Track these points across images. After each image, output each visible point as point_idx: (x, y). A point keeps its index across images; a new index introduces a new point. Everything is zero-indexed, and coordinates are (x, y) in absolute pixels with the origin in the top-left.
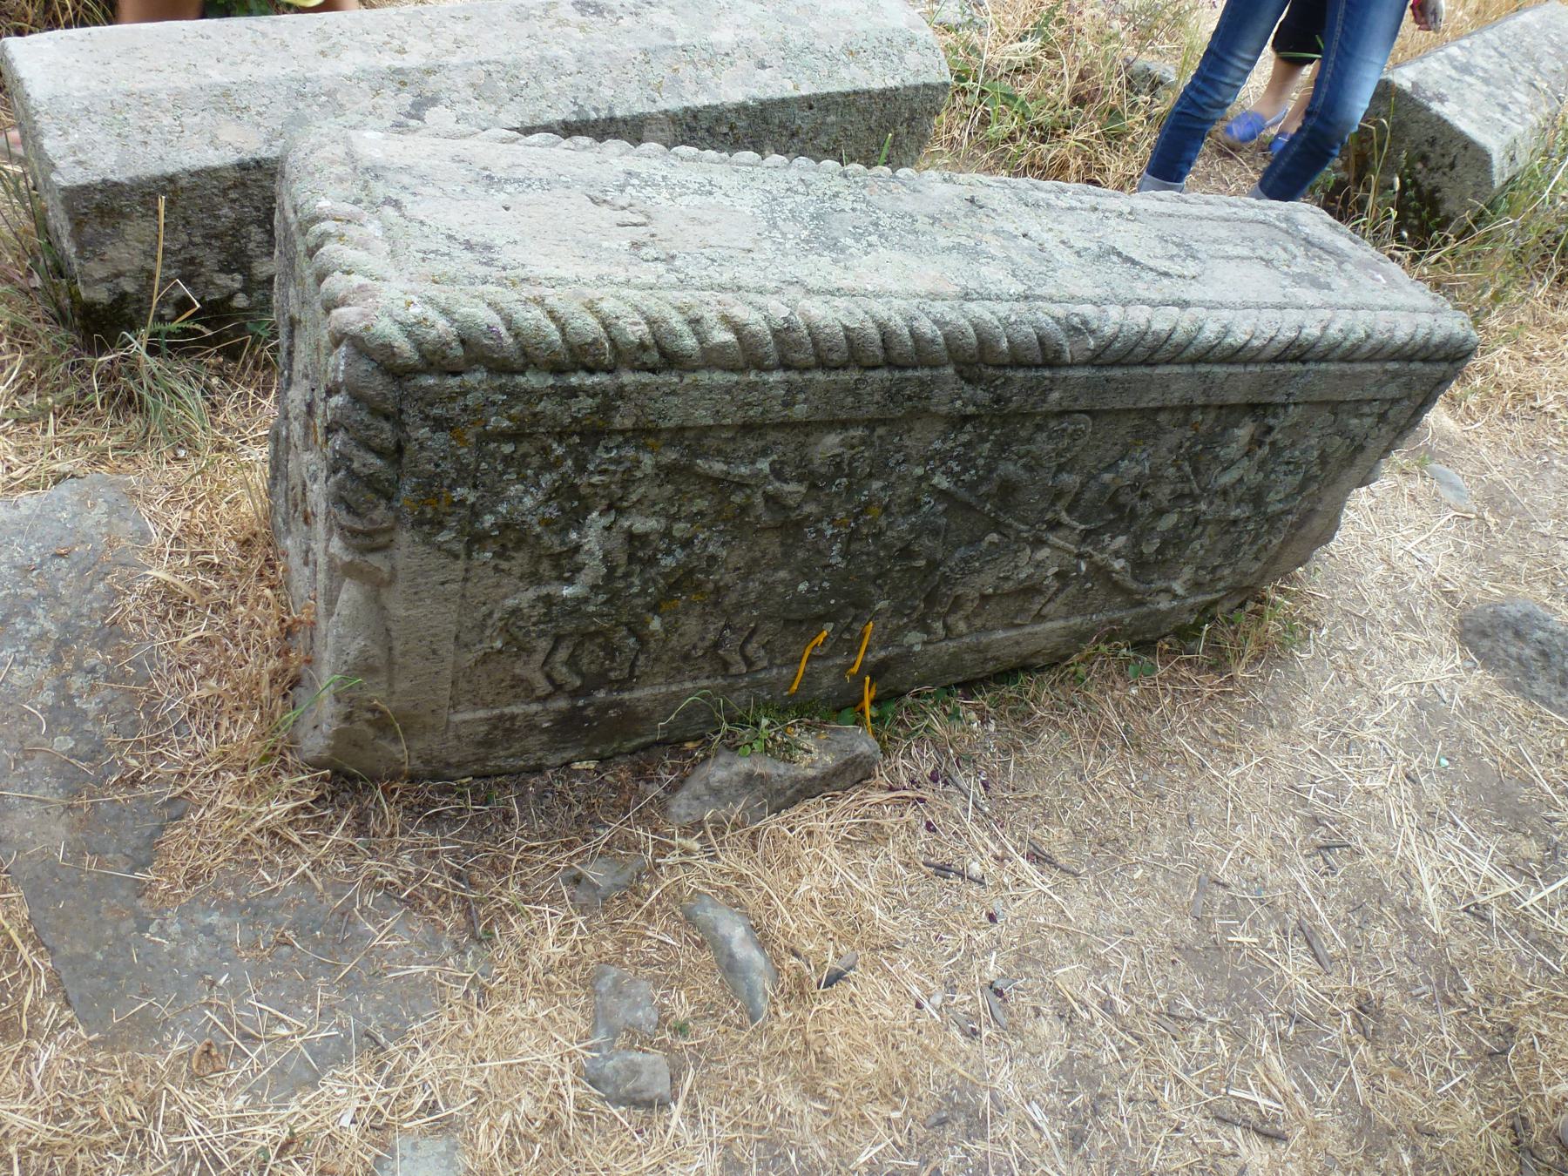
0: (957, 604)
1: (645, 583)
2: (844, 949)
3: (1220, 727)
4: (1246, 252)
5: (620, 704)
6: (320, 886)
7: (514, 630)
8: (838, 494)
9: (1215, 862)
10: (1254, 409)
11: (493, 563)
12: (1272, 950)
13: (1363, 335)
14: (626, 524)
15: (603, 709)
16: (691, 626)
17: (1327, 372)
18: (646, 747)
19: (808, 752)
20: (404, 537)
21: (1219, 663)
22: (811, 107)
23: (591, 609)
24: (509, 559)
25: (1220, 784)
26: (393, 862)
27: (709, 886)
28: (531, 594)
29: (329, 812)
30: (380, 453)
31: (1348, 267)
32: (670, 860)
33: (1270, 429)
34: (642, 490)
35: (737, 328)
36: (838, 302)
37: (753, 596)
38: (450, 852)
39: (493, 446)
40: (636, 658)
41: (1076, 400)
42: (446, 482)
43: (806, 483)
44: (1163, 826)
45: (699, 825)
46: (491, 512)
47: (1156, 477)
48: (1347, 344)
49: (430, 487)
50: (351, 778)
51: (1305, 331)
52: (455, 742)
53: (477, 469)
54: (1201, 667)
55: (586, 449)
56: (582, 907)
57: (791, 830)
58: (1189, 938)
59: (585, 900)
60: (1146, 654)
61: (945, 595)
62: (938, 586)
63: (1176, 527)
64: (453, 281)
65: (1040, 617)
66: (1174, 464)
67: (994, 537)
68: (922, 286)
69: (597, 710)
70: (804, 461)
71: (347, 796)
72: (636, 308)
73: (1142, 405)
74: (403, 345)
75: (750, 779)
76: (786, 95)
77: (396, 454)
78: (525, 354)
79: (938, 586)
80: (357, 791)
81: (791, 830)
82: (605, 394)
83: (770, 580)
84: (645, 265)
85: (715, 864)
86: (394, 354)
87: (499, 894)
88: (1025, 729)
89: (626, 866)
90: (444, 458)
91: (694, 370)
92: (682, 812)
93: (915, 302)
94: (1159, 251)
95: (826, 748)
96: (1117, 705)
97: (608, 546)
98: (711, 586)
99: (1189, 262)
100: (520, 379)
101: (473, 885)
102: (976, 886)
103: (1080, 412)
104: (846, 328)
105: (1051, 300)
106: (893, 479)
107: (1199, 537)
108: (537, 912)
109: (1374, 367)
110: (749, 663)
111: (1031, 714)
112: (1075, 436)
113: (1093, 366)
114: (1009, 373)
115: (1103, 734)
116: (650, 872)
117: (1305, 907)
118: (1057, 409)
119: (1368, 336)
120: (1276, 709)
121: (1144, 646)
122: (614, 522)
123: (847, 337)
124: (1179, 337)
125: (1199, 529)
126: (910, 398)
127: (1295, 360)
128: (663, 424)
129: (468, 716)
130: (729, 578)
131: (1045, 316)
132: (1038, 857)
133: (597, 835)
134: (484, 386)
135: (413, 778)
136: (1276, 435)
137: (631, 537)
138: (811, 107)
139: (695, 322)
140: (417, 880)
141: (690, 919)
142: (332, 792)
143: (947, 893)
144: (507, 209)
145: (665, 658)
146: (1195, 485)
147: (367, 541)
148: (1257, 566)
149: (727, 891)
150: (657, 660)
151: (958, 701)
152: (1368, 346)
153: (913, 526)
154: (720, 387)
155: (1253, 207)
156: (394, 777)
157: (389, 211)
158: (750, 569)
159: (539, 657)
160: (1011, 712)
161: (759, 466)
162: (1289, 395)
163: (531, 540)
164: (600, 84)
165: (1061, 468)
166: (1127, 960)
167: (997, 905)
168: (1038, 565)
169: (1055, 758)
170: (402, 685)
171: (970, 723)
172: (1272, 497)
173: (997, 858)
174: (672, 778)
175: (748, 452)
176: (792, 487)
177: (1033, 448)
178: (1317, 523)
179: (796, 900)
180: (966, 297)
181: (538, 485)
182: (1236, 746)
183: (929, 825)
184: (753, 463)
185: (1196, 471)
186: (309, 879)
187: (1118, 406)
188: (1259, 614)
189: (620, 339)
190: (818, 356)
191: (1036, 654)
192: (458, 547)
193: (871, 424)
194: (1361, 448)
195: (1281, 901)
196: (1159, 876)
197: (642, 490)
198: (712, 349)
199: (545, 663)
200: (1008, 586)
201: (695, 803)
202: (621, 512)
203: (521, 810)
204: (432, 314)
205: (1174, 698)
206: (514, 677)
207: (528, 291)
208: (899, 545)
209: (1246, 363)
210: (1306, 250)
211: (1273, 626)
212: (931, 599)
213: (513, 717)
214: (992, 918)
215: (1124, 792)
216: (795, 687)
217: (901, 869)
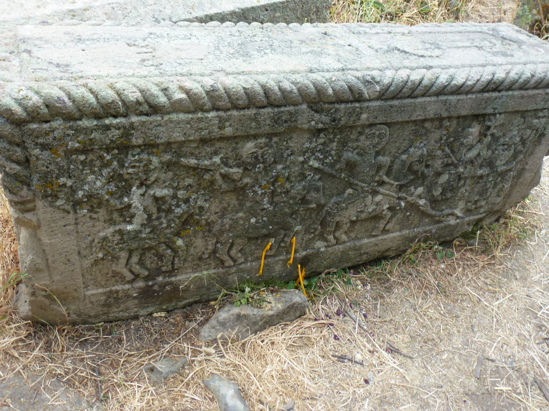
0: (338, 226)
1: (169, 221)
2: (288, 400)
3: (488, 281)
4: (468, 44)
5: (171, 283)
6: (25, 377)
7: (106, 248)
8: (260, 172)
9: (487, 349)
10: (478, 117)
11: (88, 215)
12: (520, 394)
13: (529, 75)
14: (152, 192)
15: (163, 286)
16: (199, 242)
17: (513, 96)
18: (190, 305)
19: (270, 303)
20: (40, 204)
21: (486, 250)
22: (267, 10)
23: (144, 236)
24: (96, 213)
25: (489, 309)
26: (62, 364)
27: (219, 370)
28: (111, 230)
29: (33, 341)
30: (18, 163)
31: (524, 47)
32: (199, 358)
33: (489, 128)
34: (156, 175)
35: (187, 92)
36: (241, 77)
37: (227, 226)
38: (90, 358)
39: (74, 157)
40: (174, 259)
41: (376, 118)
42: (54, 176)
43: (242, 168)
44: (459, 331)
45: (215, 340)
46: (81, 190)
47: (431, 155)
48: (521, 80)
49: (45, 177)
50: (44, 325)
51: (496, 76)
52: (90, 305)
53: (69, 168)
54: (477, 252)
55: (122, 156)
56: (154, 382)
57: (262, 341)
58: (473, 389)
59: (155, 379)
60: (449, 248)
61: (330, 221)
62: (326, 217)
63: (448, 181)
64: (46, 80)
65: (385, 231)
66: (440, 148)
67: (350, 191)
68: (287, 68)
69: (160, 286)
70: (238, 157)
71: (41, 333)
72: (135, 85)
73: (414, 118)
74: (17, 109)
75: (239, 317)
76: (254, 5)
77: (26, 162)
78: (80, 110)
79: (326, 217)
80: (47, 331)
81: (262, 341)
82: (124, 128)
83: (235, 218)
84: (145, 68)
85: (223, 360)
86: (13, 114)
87: (113, 378)
88: (386, 287)
89: (177, 362)
90: (50, 164)
91: (169, 113)
92: (206, 335)
93: (283, 75)
94: (420, 47)
95: (278, 300)
96: (433, 273)
97: (145, 204)
98: (204, 222)
99: (436, 50)
100: (80, 123)
101: (100, 374)
102: (359, 366)
103: (381, 124)
104: (244, 88)
105: (357, 70)
106: (288, 163)
107: (464, 185)
108: (131, 386)
109: (540, 91)
110: (235, 261)
111: (388, 280)
112: (381, 136)
113: (382, 100)
114: (337, 106)
115: (426, 288)
116: (189, 365)
117: (537, 370)
118: (367, 123)
119: (533, 76)
120: (519, 271)
121: (446, 244)
122: (146, 191)
123: (246, 93)
124: (425, 82)
125: (462, 182)
126: (286, 122)
127: (494, 90)
128: (159, 141)
129: (94, 292)
130: (213, 218)
131: (351, 77)
132: (391, 350)
133: (163, 347)
134: (62, 127)
135: (74, 324)
136: (493, 130)
137: (156, 199)
138: (267, 10)
139: (165, 90)
140: (73, 372)
141: (207, 387)
142: (35, 332)
143: (345, 369)
144: (83, 50)
145: (189, 259)
146: (454, 159)
147: (22, 207)
148: (499, 200)
149: (228, 373)
150: (185, 260)
151: (350, 275)
152: (533, 81)
153: (304, 188)
154: (183, 121)
155: (476, 26)
156: (64, 323)
157: (25, 55)
158: (223, 214)
159: (123, 261)
160: (378, 279)
161: (214, 160)
162: (494, 109)
163: (105, 203)
164: (165, 8)
165: (378, 154)
166: (439, 401)
167: (370, 375)
168: (377, 204)
169: (402, 301)
170: (56, 278)
171: (357, 285)
172: (498, 163)
173: (370, 351)
174: (202, 318)
175: (207, 153)
176: (235, 170)
177: (360, 144)
178: (528, 176)
179: (264, 376)
180: (311, 71)
181: (102, 175)
182: (497, 290)
183: (335, 336)
184: (211, 159)
185: (453, 151)
186: (21, 374)
187: (400, 120)
188: (506, 224)
189: (127, 100)
190: (232, 103)
191: (388, 250)
192: (68, 207)
193: (270, 136)
194: (543, 135)
195: (524, 368)
196: (456, 357)
197: (156, 175)
199: (127, 264)
200: (363, 216)
201: (213, 330)
202: (148, 187)
203: (127, 337)
204: (31, 94)
205: (464, 269)
206: (113, 272)
207: (83, 81)
208: (299, 197)
209: (467, 93)
210: (502, 42)
211: (514, 230)
212: (323, 224)
213: (117, 292)
214: (366, 381)
215: (437, 315)
216: (261, 271)
217: (320, 359)
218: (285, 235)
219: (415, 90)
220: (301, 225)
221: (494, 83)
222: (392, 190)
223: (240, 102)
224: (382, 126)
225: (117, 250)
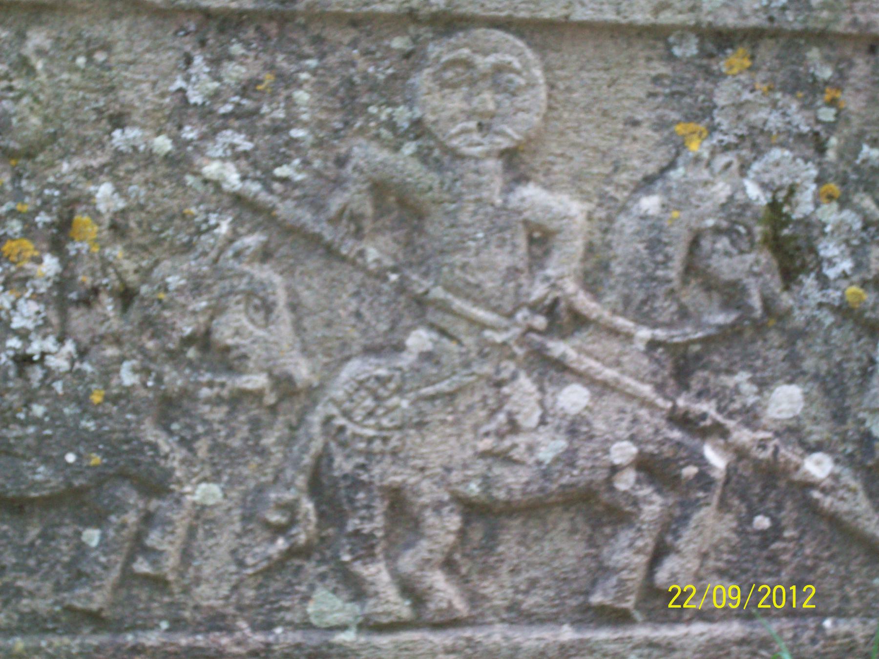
103: (495, 24)
218: (148, 519)
220: (215, 477)
222: (630, 367)
224: (498, 35)
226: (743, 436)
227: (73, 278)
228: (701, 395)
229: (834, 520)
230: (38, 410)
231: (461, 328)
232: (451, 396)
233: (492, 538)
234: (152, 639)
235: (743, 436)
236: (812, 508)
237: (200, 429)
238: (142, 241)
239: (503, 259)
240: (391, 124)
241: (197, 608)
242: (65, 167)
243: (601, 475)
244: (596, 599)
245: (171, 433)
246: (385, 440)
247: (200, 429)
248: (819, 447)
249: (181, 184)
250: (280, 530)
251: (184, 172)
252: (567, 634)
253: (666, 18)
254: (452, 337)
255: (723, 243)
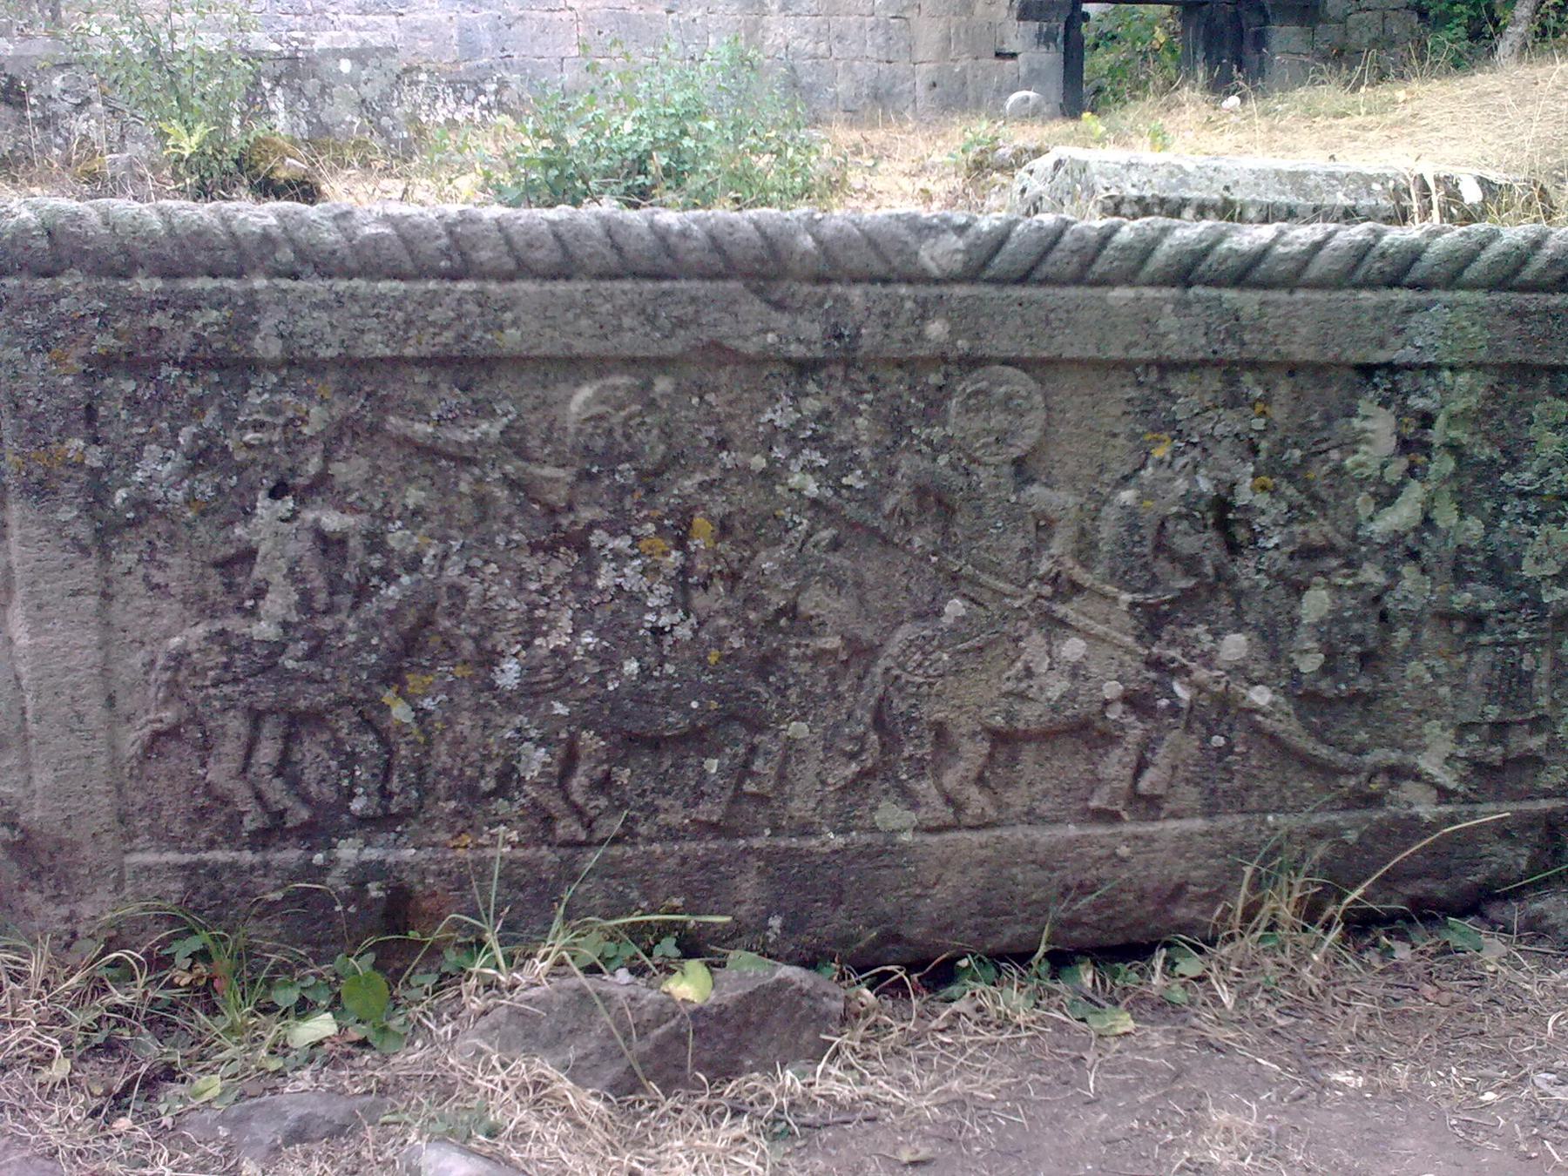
24: (162, 566)
28: (201, 630)
33: (1427, 419)
125: (1402, 635)
129: (150, 858)
146: (1327, 528)
192: (84, 532)
198: (363, 244)
219: (1093, 261)
220: (803, 717)
221: (1383, 255)
222: (1115, 623)
223: (539, 255)
224: (1009, 370)
225: (217, 704)
226: (1201, 674)
227: (694, 566)
228: (1172, 643)
229: (1273, 738)
230: (670, 669)
231: (987, 595)
232: (981, 649)
233: (1014, 759)
234: (757, 843)
235: (1201, 674)
236: (1257, 729)
237: (791, 681)
238: (746, 537)
239: (1019, 542)
240: (929, 443)
241: (791, 818)
242: (687, 483)
243: (1096, 707)
244: (1094, 804)
245: (769, 684)
246: (931, 685)
247: (791, 681)
248: (1260, 682)
249: (772, 492)
250: (852, 756)
251: (774, 484)
252: (1072, 830)
253: (1135, 353)
254: (980, 604)
255: (1183, 526)
